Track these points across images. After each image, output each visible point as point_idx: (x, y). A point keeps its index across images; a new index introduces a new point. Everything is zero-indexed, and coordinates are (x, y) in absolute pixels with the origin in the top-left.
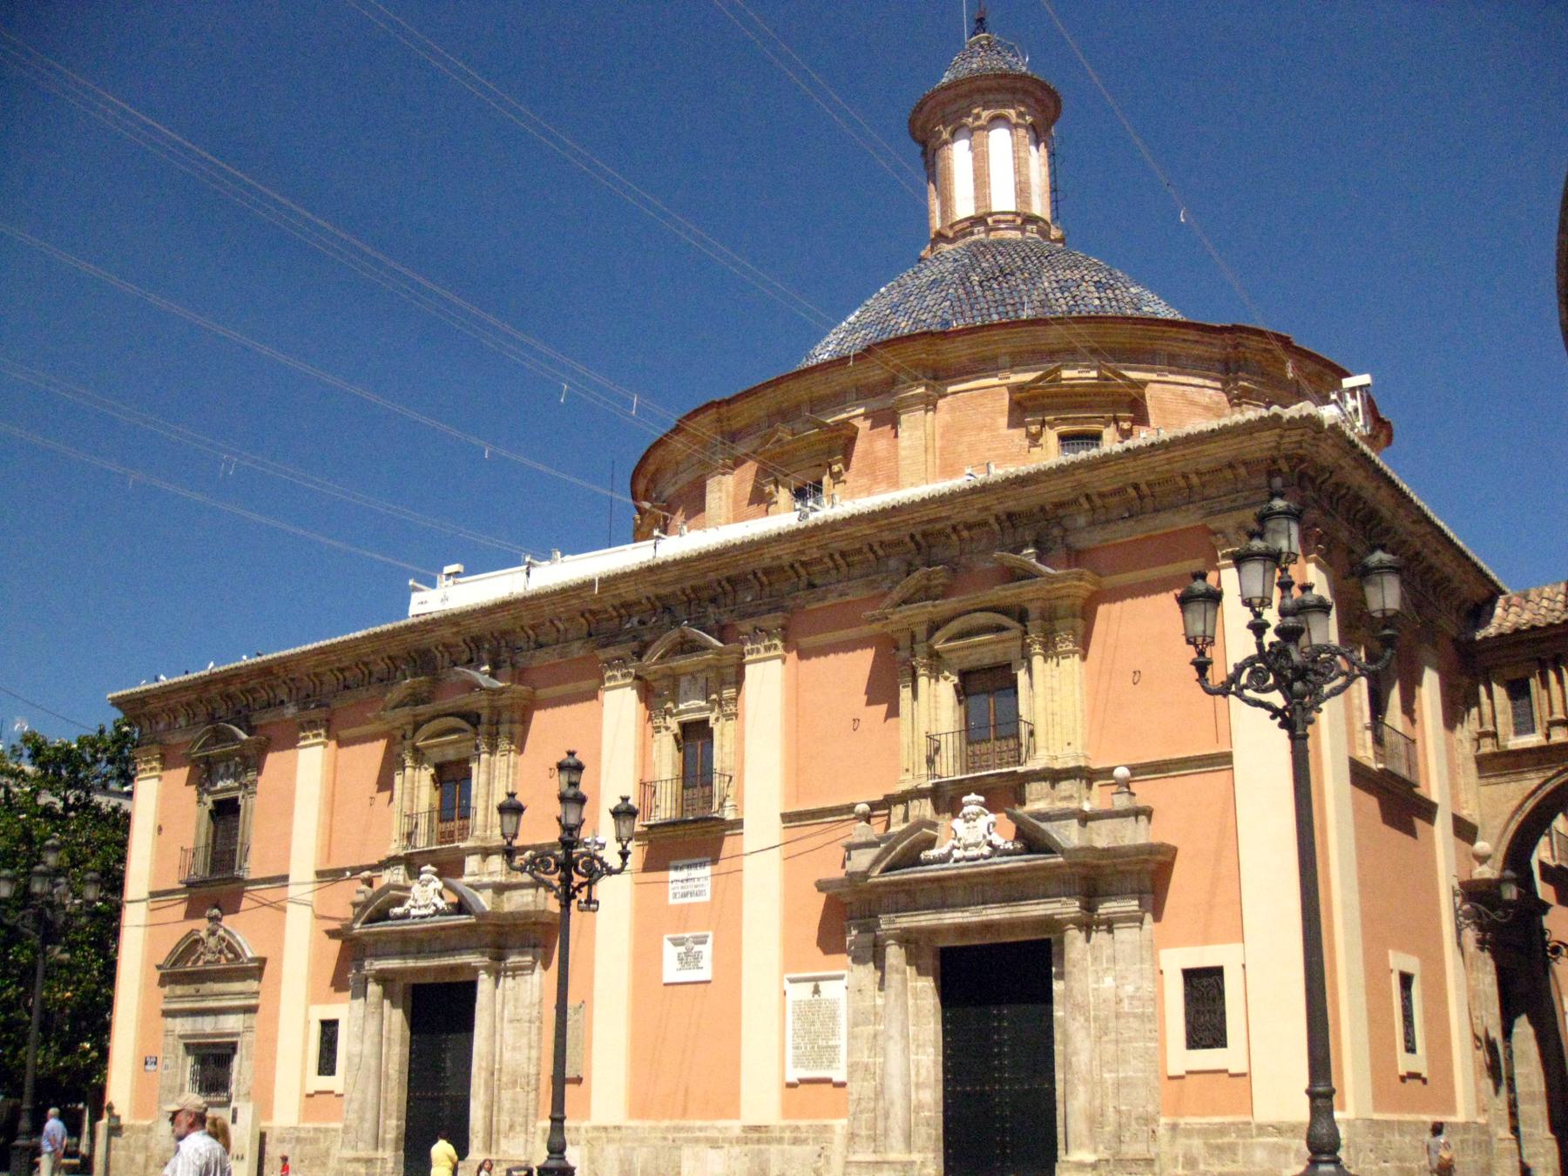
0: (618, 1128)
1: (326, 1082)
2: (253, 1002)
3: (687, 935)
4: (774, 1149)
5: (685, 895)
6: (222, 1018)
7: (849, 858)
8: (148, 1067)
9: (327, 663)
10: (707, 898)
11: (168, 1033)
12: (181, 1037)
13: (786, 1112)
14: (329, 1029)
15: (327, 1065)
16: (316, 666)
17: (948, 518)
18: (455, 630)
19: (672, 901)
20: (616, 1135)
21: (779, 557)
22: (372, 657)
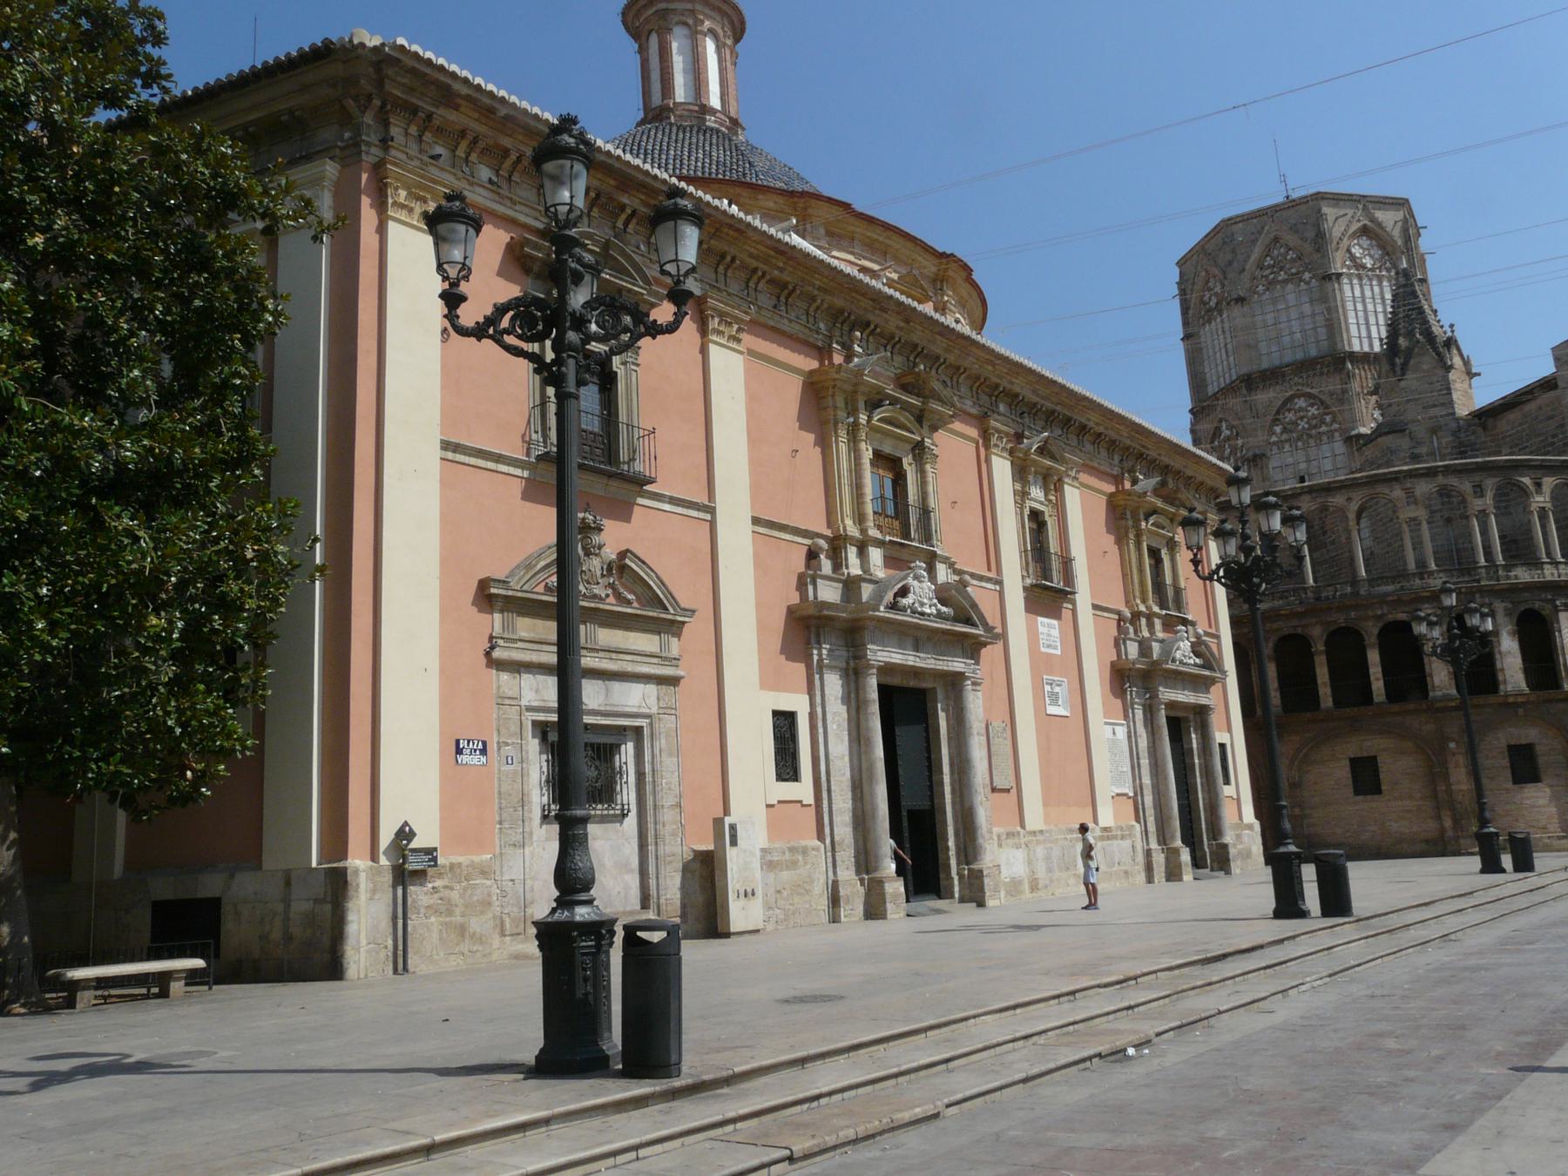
0: (1041, 832)
1: (789, 790)
2: (680, 673)
3: (1055, 678)
4: (1115, 842)
5: (1049, 646)
6: (617, 687)
7: (1117, 645)
8: (464, 759)
9: (766, 262)
10: (1058, 652)
11: (502, 701)
12: (530, 709)
13: (1116, 816)
14: (784, 723)
15: (787, 767)
16: (751, 256)
17: (1148, 449)
18: (902, 324)
19: (1043, 650)
20: (1040, 838)
21: (1089, 420)
22: (816, 292)
